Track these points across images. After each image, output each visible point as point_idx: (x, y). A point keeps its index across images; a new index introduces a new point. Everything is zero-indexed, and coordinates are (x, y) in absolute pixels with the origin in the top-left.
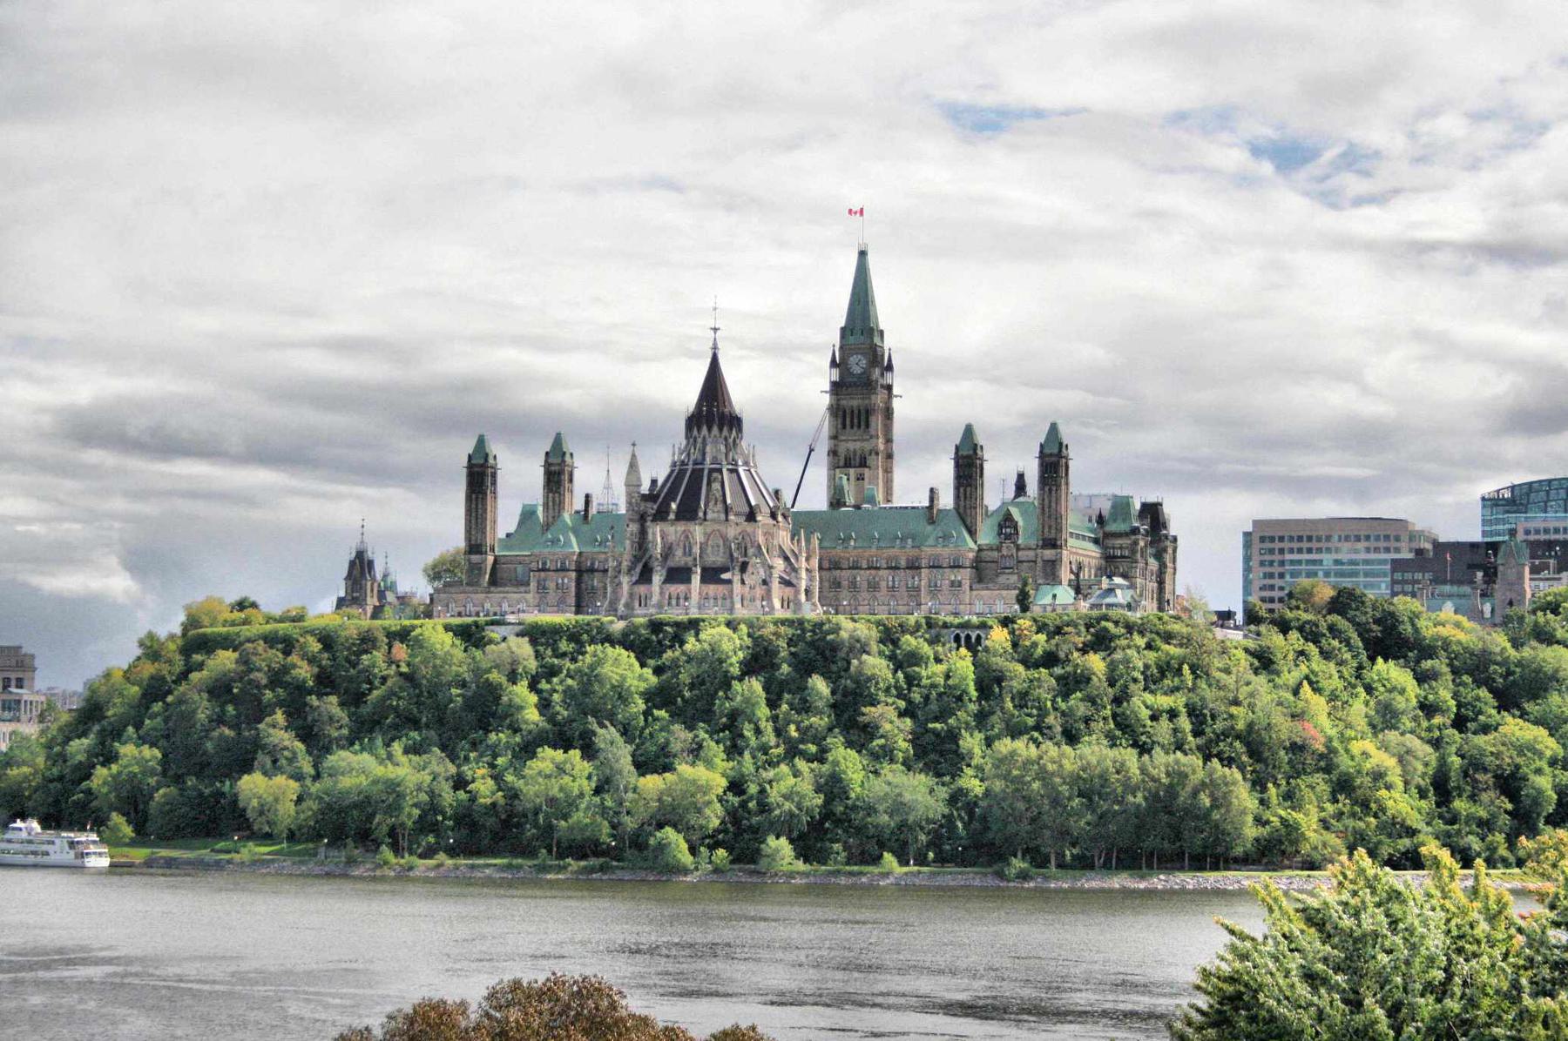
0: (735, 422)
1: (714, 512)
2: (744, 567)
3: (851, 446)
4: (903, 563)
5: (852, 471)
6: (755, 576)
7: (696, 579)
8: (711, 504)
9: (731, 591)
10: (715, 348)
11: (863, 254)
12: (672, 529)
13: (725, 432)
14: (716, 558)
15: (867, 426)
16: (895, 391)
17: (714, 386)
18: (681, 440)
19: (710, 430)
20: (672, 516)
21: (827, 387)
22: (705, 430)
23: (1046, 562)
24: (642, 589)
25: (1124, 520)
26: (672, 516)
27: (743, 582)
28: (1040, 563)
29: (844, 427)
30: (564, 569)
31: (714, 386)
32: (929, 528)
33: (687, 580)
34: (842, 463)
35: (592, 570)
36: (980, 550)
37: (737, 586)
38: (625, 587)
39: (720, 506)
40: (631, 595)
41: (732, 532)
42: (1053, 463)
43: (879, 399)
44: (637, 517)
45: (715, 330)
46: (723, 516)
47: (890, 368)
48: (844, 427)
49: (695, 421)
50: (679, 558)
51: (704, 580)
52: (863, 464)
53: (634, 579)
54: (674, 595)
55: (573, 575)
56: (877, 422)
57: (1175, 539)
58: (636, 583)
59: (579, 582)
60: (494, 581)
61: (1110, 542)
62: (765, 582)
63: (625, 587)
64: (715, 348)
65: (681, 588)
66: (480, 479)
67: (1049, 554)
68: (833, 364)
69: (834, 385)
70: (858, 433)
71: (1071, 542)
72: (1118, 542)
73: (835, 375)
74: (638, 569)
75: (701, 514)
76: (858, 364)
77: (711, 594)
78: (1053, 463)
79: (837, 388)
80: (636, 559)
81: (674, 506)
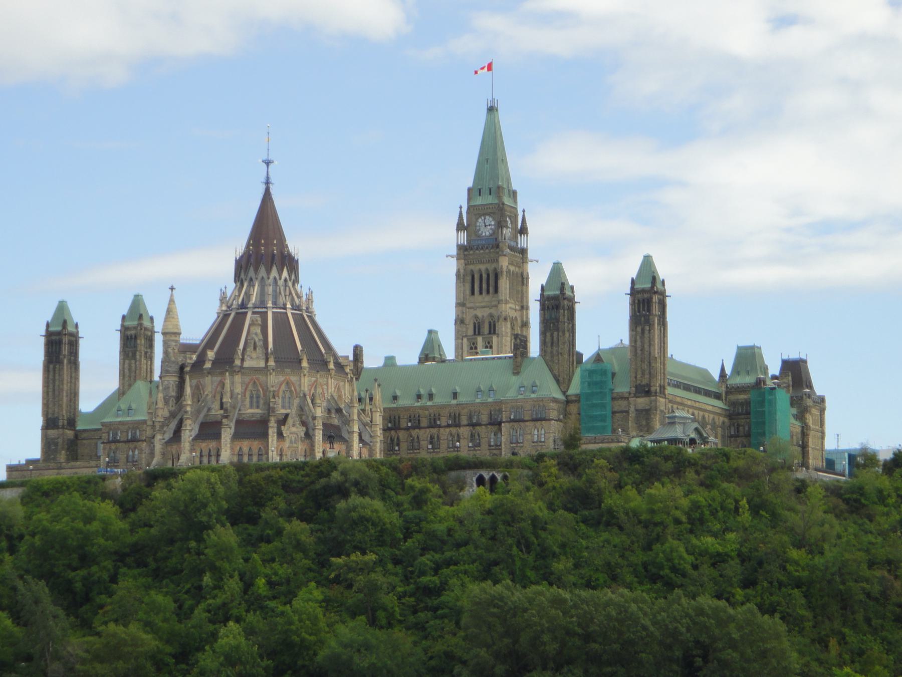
0: (289, 263)
2: (283, 421)
3: (479, 313)
4: (485, 419)
5: (480, 340)
6: (293, 430)
7: (227, 434)
8: (250, 349)
10: (267, 183)
12: (208, 380)
13: (274, 273)
14: (252, 412)
15: (496, 290)
16: (530, 255)
18: (231, 286)
19: (256, 270)
20: (208, 365)
21: (454, 251)
22: (251, 273)
23: (639, 412)
24: (174, 448)
25: (748, 373)
26: (208, 365)
27: (280, 435)
28: (632, 414)
29: (473, 293)
32: (514, 378)
33: (217, 437)
34: (470, 332)
36: (568, 402)
38: (158, 447)
39: (259, 350)
40: (163, 454)
41: (273, 380)
42: (647, 302)
43: (504, 262)
44: (175, 368)
45: (268, 163)
46: (262, 364)
48: (473, 293)
49: (245, 267)
51: (236, 436)
52: (493, 330)
53: (168, 435)
54: (205, 453)
57: (822, 400)
61: (733, 397)
63: (158, 447)
64: (267, 183)
65: (212, 444)
67: (642, 402)
69: (460, 247)
70: (486, 298)
71: (669, 390)
72: (742, 397)
74: (173, 425)
75: (238, 362)
76: (486, 225)
77: (246, 450)
78: (647, 302)
79: (464, 251)
80: (173, 415)
81: (211, 354)
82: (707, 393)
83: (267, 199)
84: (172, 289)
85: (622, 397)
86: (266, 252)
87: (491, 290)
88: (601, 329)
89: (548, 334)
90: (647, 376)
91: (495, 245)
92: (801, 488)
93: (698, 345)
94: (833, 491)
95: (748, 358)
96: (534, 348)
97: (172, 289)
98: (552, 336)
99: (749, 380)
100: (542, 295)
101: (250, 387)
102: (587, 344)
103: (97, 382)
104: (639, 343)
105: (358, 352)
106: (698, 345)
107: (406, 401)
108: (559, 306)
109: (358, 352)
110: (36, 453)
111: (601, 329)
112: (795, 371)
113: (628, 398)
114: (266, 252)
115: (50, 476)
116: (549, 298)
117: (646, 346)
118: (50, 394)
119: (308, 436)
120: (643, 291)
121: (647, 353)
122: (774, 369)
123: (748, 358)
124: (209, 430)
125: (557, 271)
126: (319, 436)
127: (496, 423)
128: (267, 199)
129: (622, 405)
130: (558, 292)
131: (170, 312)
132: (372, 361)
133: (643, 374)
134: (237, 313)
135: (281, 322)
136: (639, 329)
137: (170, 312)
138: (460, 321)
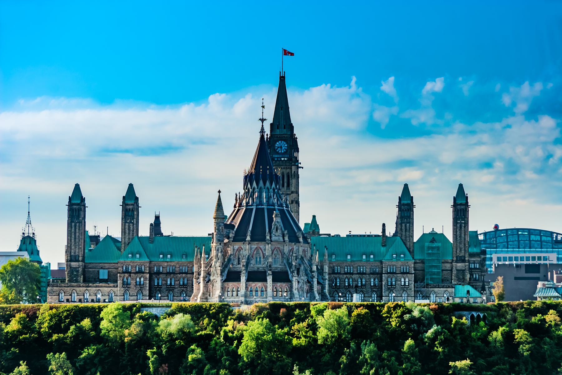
1: (277, 236)
7: (270, 279)
9: (291, 287)
15: (288, 185)
24: (231, 285)
26: (248, 238)
30: (140, 272)
32: (383, 249)
35: (158, 273)
37: (295, 285)
46: (281, 239)
50: (254, 266)
53: (224, 278)
55: (148, 275)
56: (293, 181)
58: (225, 281)
59: (151, 280)
60: (84, 281)
62: (308, 282)
65: (259, 284)
67: (460, 265)
75: (268, 237)
84: (219, 192)
87: (285, 184)
89: (403, 225)
90: (463, 252)
97: (219, 192)
98: (406, 226)
100: (400, 202)
101: (275, 252)
104: (458, 233)
113: (451, 263)
116: (404, 205)
117: (463, 235)
118: (73, 240)
120: (461, 204)
121: (463, 239)
129: (448, 266)
130: (409, 202)
133: (461, 250)
134: (257, 209)
136: (458, 225)
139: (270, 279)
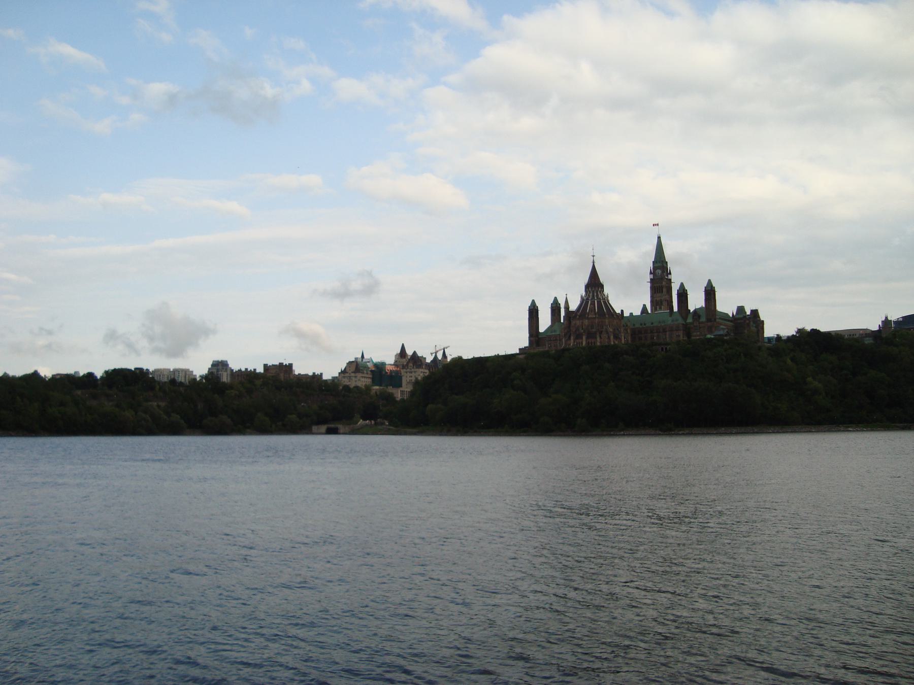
0: (602, 286)
2: (601, 333)
6: (604, 335)
7: (584, 338)
11: (659, 238)
17: (594, 274)
18: (584, 294)
31: (594, 274)
37: (598, 339)
42: (710, 293)
43: (664, 283)
47: (670, 273)
49: (587, 287)
51: (587, 338)
56: (664, 290)
66: (533, 312)
67: (709, 324)
68: (651, 273)
73: (652, 276)
78: (710, 293)
79: (652, 281)
82: (729, 321)
83: (594, 267)
85: (702, 323)
86: (594, 284)
88: (696, 301)
91: (662, 278)
92: (760, 348)
93: (726, 305)
94: (768, 349)
95: (741, 309)
96: (675, 309)
99: (741, 316)
102: (692, 307)
103: (545, 322)
105: (622, 311)
106: (726, 305)
107: (637, 326)
108: (683, 295)
109: (622, 311)
110: (527, 344)
111: (696, 301)
112: (755, 313)
114: (594, 284)
115: (532, 351)
119: (609, 338)
122: (748, 313)
123: (741, 309)
124: (579, 336)
125: (682, 285)
126: (612, 337)
127: (664, 331)
128: (594, 267)
131: (567, 302)
132: (626, 314)
135: (599, 303)
137: (567, 302)
138: (652, 302)
139: (584, 338)
